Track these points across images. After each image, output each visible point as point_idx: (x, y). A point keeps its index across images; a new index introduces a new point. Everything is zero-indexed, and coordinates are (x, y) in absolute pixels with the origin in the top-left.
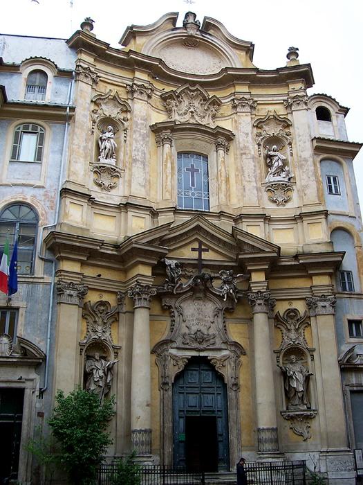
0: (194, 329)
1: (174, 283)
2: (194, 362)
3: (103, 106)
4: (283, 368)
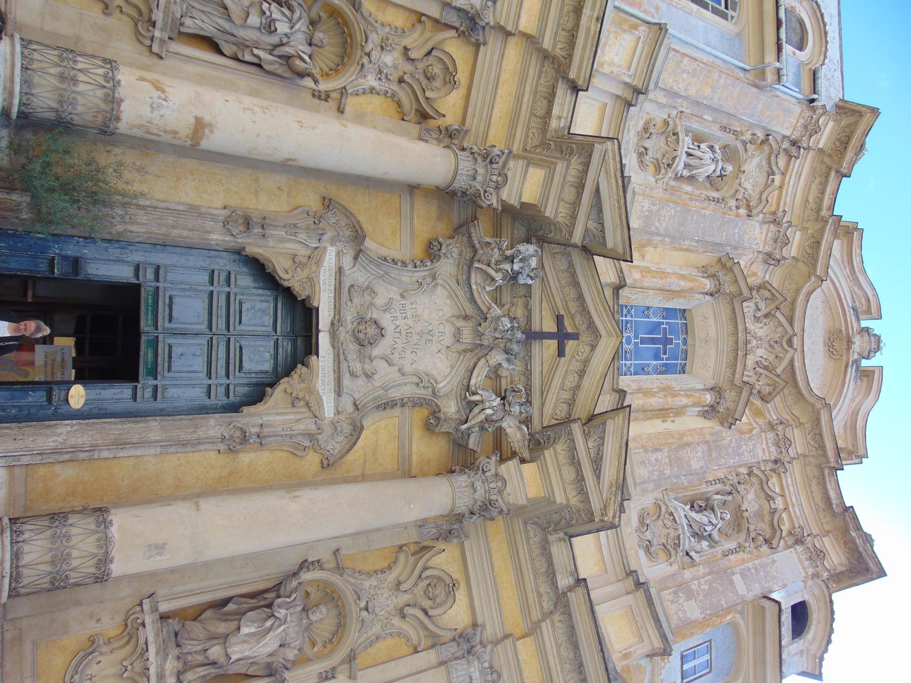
0: (386, 321)
1: (497, 263)
2: (300, 317)
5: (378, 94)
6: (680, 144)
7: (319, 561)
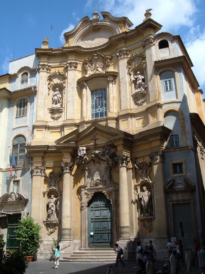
1: (82, 158)
3: (54, 80)
5: (58, 185)
6: (54, 108)
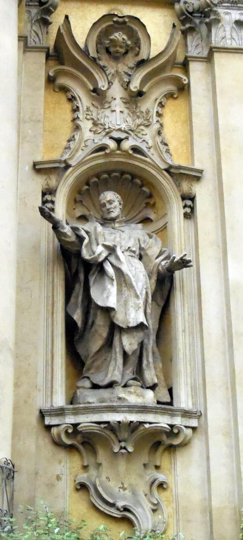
4: (67, 230)
7: (44, 194)
